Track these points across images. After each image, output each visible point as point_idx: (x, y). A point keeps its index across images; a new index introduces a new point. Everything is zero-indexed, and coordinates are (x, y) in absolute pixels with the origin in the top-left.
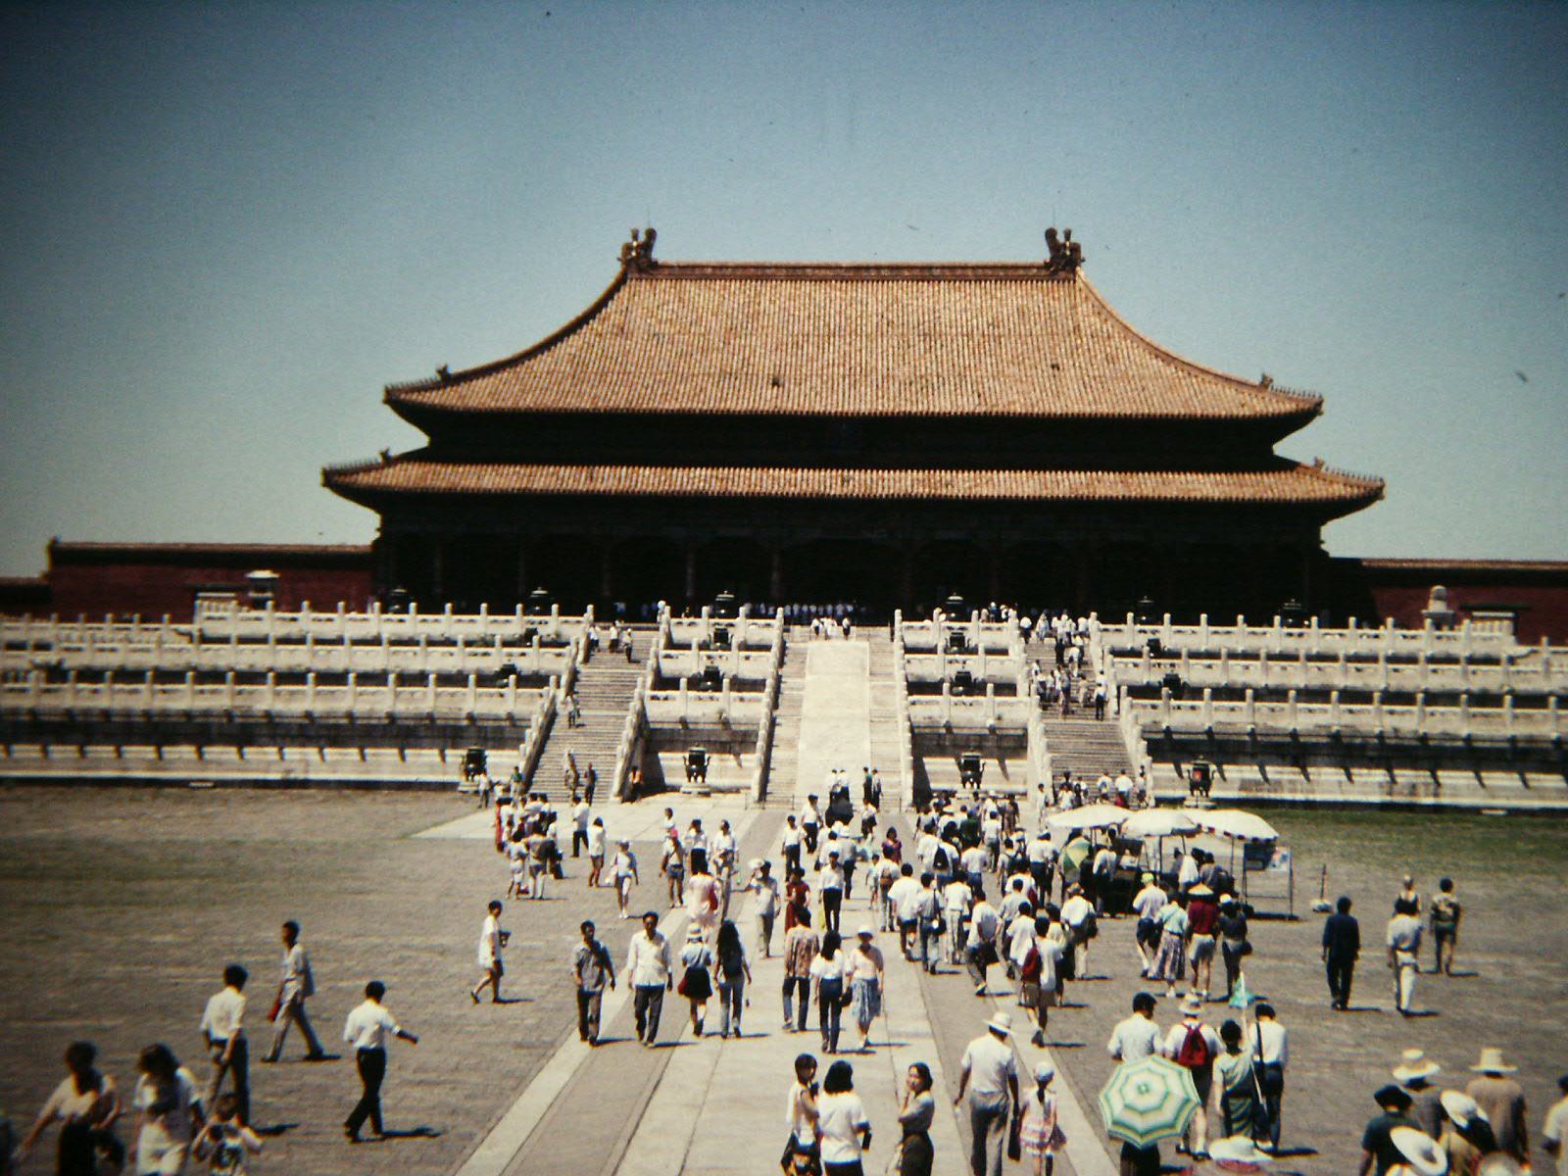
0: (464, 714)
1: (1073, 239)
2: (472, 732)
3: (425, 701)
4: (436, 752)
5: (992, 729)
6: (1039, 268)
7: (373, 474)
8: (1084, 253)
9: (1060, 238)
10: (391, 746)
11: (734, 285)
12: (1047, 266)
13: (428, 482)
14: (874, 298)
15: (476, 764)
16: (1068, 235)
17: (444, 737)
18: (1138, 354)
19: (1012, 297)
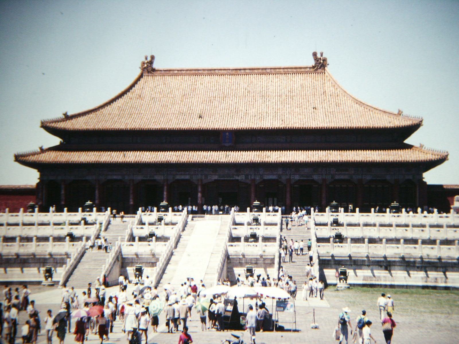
0: (47, 253)
1: (324, 56)
2: (51, 260)
3: (32, 248)
4: (36, 269)
5: (261, 256)
6: (310, 68)
7: (36, 156)
8: (328, 61)
9: (319, 56)
10: (17, 267)
11: (187, 78)
12: (313, 67)
13: (58, 158)
14: (242, 81)
15: (49, 273)
16: (322, 55)
17: (40, 263)
18: (349, 102)
19: (299, 79)
